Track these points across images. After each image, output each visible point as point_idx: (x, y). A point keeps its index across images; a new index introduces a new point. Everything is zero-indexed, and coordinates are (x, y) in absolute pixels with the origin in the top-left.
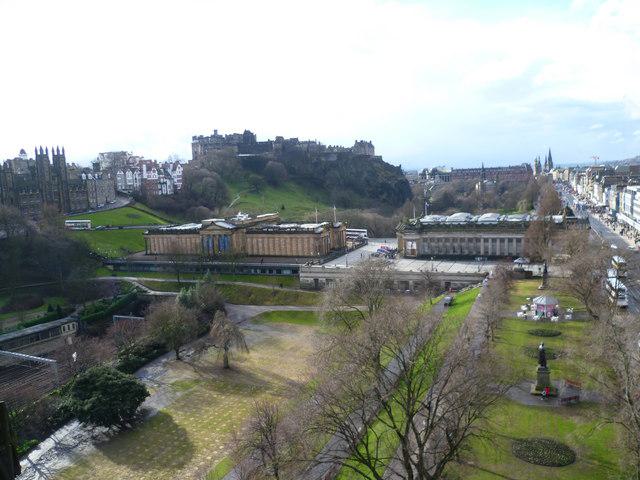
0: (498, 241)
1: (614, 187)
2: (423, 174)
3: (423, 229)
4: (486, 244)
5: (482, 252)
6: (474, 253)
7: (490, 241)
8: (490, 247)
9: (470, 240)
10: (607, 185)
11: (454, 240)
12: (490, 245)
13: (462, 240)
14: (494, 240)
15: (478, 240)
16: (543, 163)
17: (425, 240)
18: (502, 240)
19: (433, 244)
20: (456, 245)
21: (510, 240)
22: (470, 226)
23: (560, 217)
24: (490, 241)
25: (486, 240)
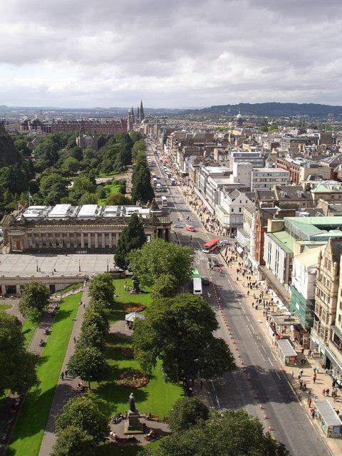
0: (96, 235)
1: (193, 158)
2: (25, 124)
3: (28, 223)
4: (86, 238)
5: (83, 246)
6: (75, 246)
7: (89, 235)
8: (89, 241)
9: (71, 235)
10: (186, 155)
11: (57, 235)
12: (89, 238)
13: (64, 235)
14: (92, 235)
15: (78, 235)
16: (135, 113)
17: (29, 235)
18: (100, 235)
19: (37, 238)
20: (58, 239)
21: (107, 235)
22: (71, 220)
23: (147, 211)
24: (89, 235)
25: (85, 235)
